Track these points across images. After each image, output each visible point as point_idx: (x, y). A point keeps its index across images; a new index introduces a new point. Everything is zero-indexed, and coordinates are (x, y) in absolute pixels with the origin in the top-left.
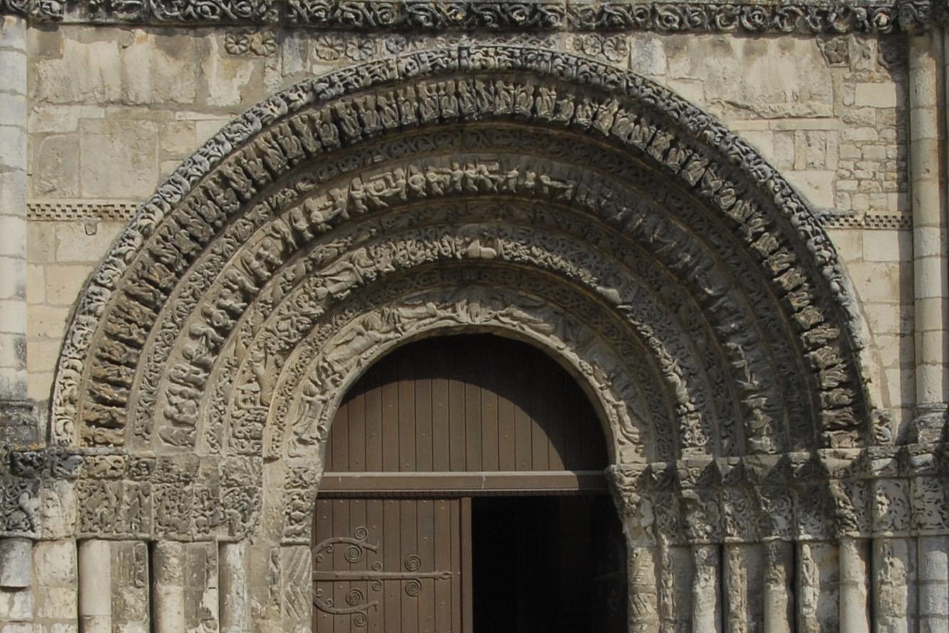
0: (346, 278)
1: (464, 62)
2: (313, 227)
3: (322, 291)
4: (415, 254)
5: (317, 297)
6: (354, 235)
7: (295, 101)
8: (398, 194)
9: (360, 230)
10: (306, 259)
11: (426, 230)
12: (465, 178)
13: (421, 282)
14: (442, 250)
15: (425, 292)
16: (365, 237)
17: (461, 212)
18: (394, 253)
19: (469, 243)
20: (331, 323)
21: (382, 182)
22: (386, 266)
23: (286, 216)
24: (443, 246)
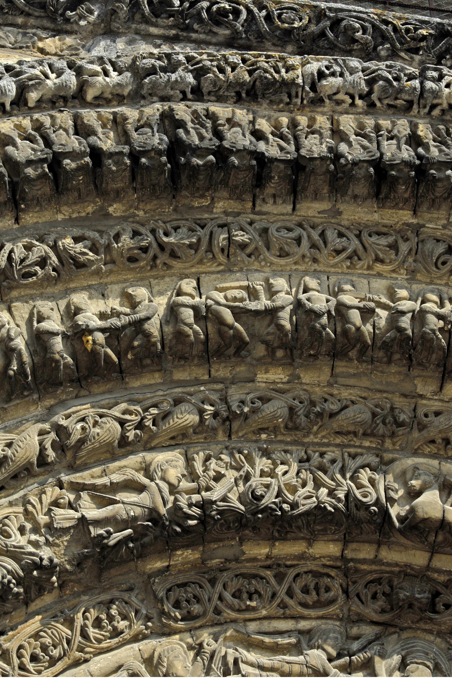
0: (130, 504)
1: (429, 84)
2: (77, 334)
3: (65, 517)
4: (294, 490)
5: (49, 526)
6: (166, 406)
7: (96, 74)
8: (272, 313)
9: (177, 402)
10: (47, 426)
11: (322, 455)
12: (419, 317)
13: (297, 590)
14: (358, 493)
15: (304, 625)
16: (187, 417)
17: (402, 417)
18: (247, 478)
19: (419, 494)
20: (70, 623)
21: (244, 294)
22: (226, 491)
23: (22, 310)
24: (360, 486)
